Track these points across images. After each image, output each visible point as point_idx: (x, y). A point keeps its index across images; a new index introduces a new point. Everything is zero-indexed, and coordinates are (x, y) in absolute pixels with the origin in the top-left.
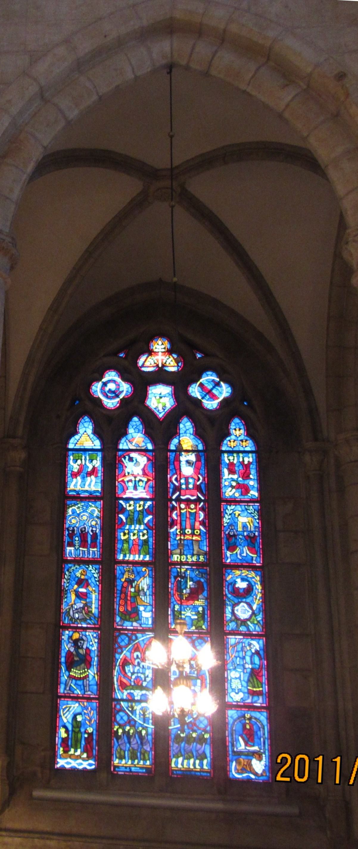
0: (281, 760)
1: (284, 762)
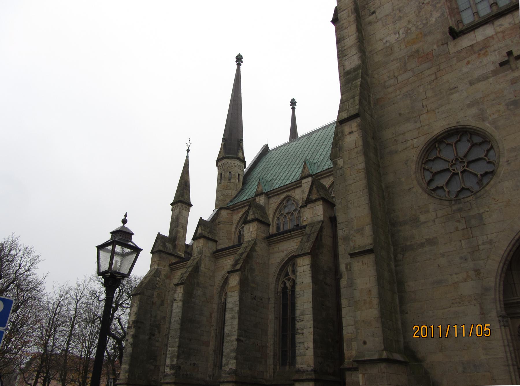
0: (415, 328)
1: (416, 330)
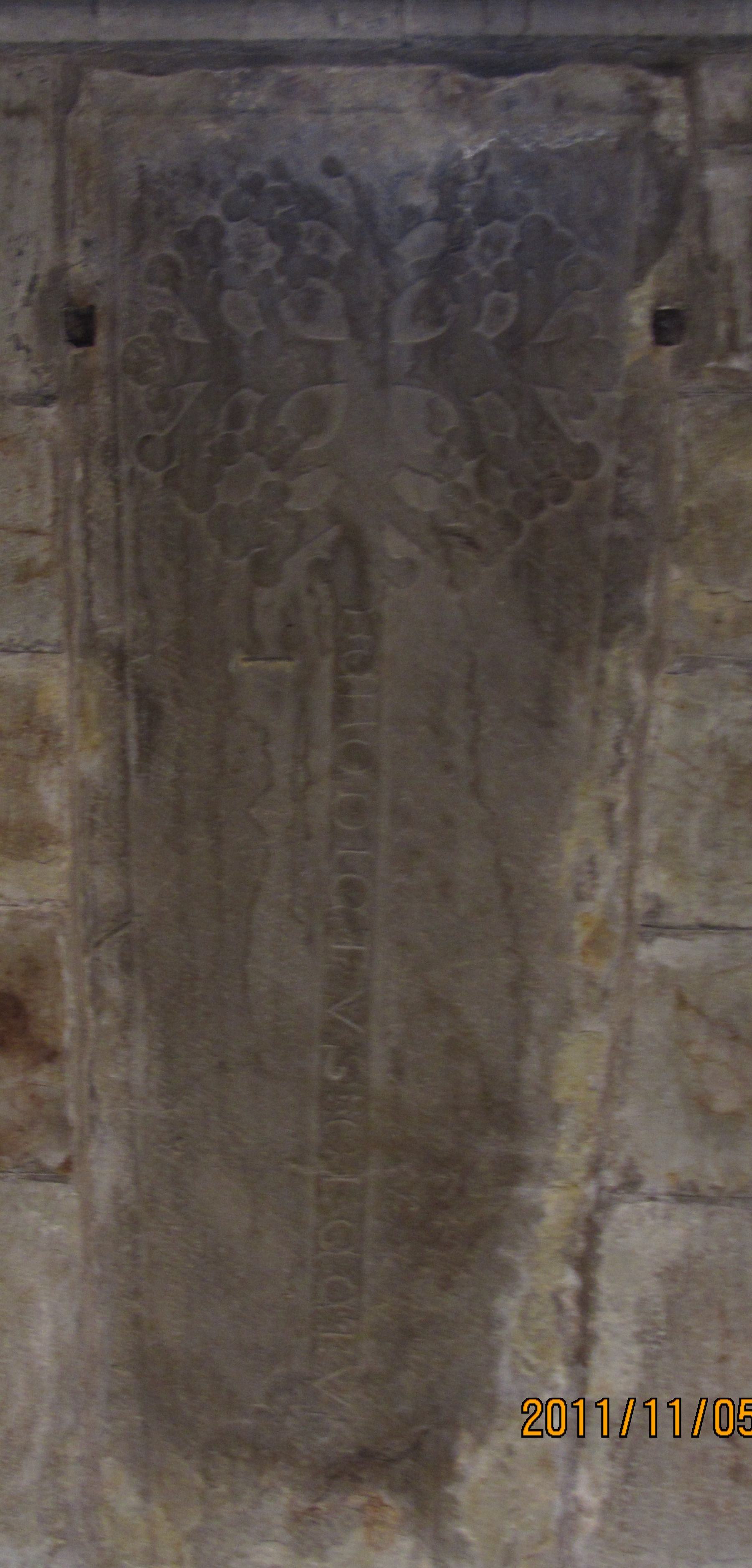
1: (532, 1409)
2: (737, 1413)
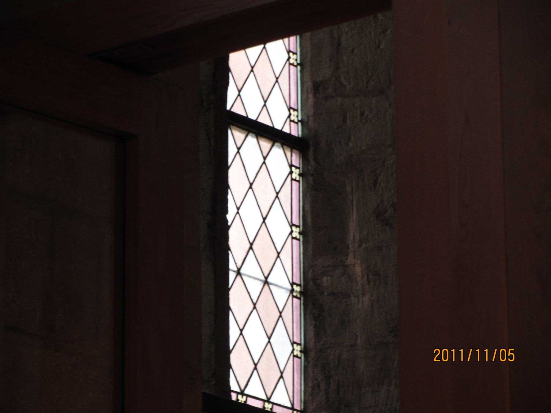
0: (436, 352)
2: (507, 353)
